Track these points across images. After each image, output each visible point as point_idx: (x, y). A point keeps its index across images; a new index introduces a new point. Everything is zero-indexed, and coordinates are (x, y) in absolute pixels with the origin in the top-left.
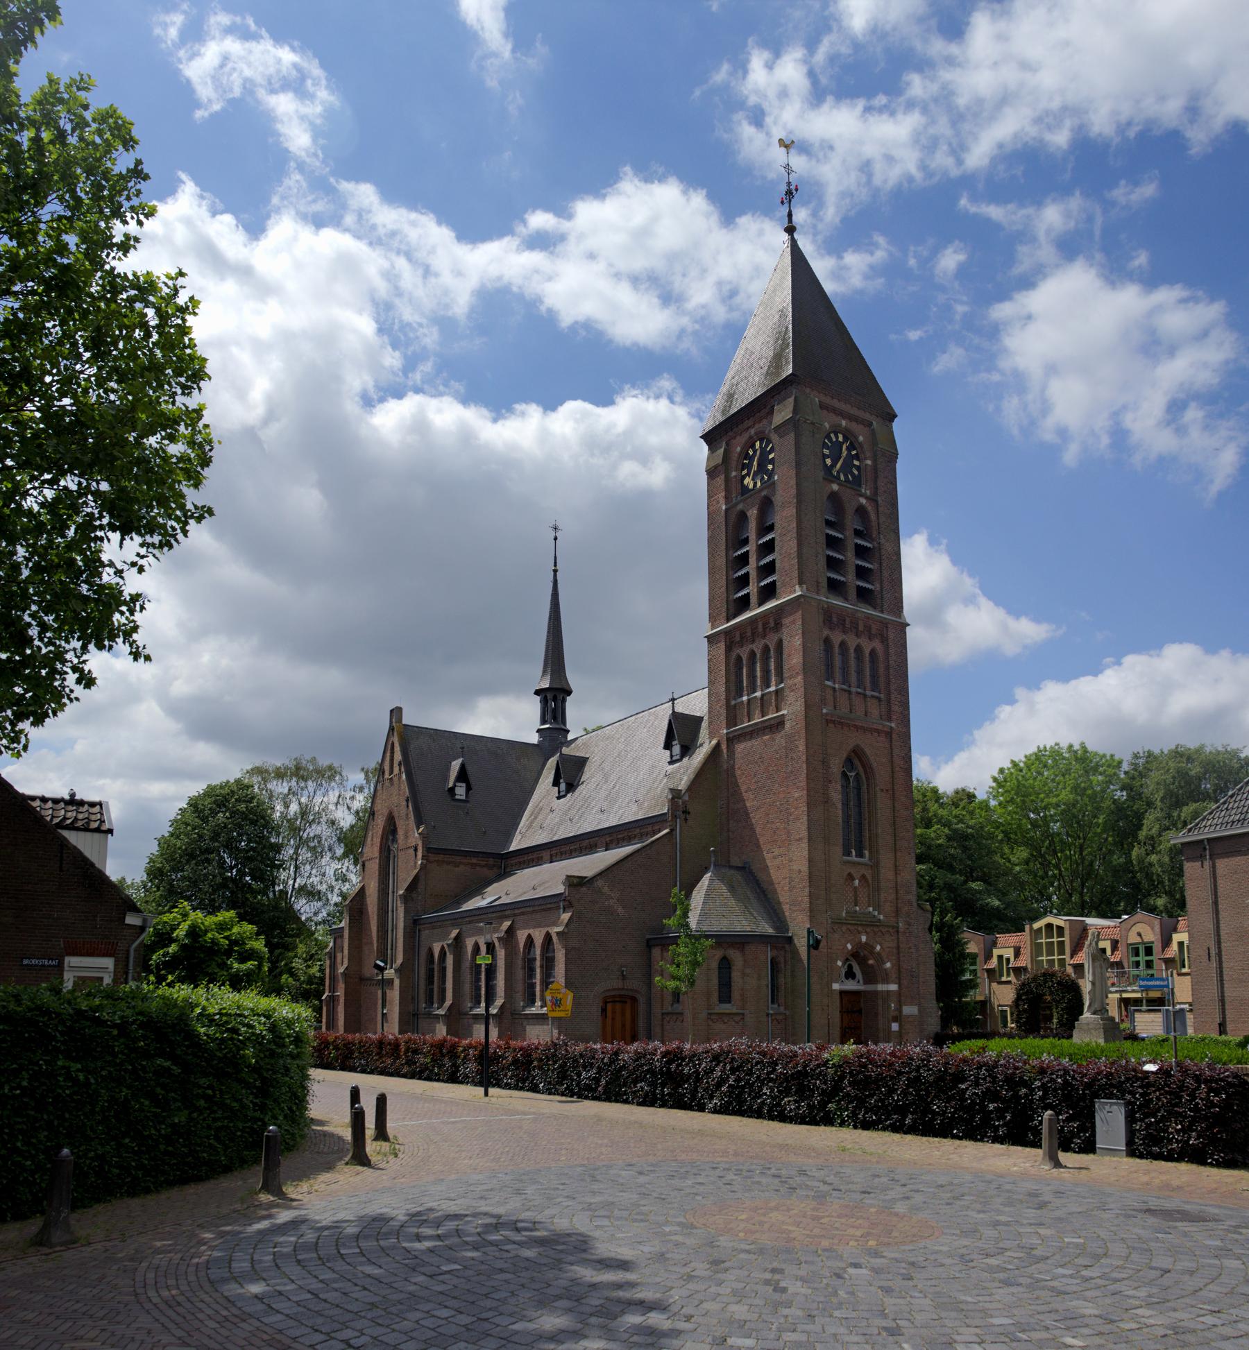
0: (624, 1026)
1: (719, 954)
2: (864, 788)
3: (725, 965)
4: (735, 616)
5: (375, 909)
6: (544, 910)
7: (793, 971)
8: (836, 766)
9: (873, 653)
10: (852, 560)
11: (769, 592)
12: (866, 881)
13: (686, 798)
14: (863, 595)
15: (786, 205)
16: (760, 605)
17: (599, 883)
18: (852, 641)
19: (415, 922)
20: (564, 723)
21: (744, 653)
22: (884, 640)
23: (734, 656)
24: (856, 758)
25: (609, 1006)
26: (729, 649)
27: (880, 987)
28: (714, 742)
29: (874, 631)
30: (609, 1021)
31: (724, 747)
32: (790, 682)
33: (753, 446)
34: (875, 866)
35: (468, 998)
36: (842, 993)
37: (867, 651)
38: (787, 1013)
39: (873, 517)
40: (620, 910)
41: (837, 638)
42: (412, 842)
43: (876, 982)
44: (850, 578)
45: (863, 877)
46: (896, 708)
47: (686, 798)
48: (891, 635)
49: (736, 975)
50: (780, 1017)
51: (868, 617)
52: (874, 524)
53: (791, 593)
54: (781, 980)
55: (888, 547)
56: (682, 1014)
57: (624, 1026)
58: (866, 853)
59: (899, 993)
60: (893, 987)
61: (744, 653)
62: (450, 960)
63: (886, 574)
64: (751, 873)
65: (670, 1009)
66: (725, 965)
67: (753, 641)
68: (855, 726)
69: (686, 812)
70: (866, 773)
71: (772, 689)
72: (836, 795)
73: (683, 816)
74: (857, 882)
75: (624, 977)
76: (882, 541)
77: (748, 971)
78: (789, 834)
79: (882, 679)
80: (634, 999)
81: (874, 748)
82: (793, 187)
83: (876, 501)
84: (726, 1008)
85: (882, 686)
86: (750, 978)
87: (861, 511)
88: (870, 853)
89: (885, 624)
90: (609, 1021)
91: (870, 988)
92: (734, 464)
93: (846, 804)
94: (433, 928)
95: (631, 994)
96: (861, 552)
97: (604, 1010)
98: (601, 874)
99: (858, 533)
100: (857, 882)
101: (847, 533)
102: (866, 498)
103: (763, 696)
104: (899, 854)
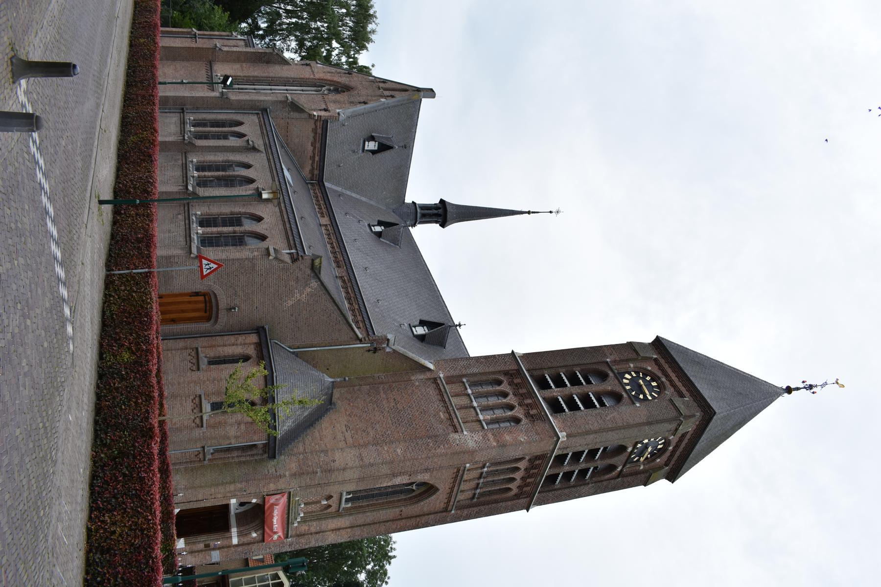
0: (183, 311)
2: (403, 497)
4: (531, 376)
5: (272, 75)
6: (286, 233)
7: (244, 462)
9: (510, 489)
11: (556, 407)
13: (388, 350)
15: (802, 385)
16: (544, 399)
17: (314, 284)
18: (518, 475)
19: (265, 110)
20: (421, 223)
21: (505, 387)
22: (517, 496)
23: (502, 378)
25: (201, 298)
26: (506, 373)
27: (234, 531)
28: (431, 366)
30: (186, 299)
31: (428, 375)
32: (490, 436)
33: (653, 380)
34: (338, 514)
35: (201, 159)
36: (227, 506)
38: (206, 462)
40: (290, 303)
42: (331, 107)
43: (239, 525)
44: (566, 468)
45: (329, 506)
46: (466, 512)
50: (201, 456)
52: (603, 478)
53: (559, 428)
54: (235, 454)
55: (585, 489)
56: (198, 369)
57: (183, 311)
58: (350, 505)
59: (230, 546)
60: (235, 541)
61: (505, 387)
62: (233, 142)
64: (327, 410)
65: (201, 355)
67: (515, 395)
69: (375, 350)
70: (416, 497)
71: (481, 417)
75: (229, 309)
76: (590, 485)
77: (243, 427)
78: (365, 445)
79: (488, 498)
80: (209, 319)
81: (436, 501)
82: (814, 390)
83: (618, 477)
85: (482, 499)
87: (613, 467)
90: (186, 299)
91: (233, 520)
92: (639, 365)
94: (261, 126)
95: (214, 315)
96: (583, 473)
97: (197, 294)
98: (322, 284)
99: (595, 468)
102: (622, 470)
103: (474, 408)
104: (349, 530)
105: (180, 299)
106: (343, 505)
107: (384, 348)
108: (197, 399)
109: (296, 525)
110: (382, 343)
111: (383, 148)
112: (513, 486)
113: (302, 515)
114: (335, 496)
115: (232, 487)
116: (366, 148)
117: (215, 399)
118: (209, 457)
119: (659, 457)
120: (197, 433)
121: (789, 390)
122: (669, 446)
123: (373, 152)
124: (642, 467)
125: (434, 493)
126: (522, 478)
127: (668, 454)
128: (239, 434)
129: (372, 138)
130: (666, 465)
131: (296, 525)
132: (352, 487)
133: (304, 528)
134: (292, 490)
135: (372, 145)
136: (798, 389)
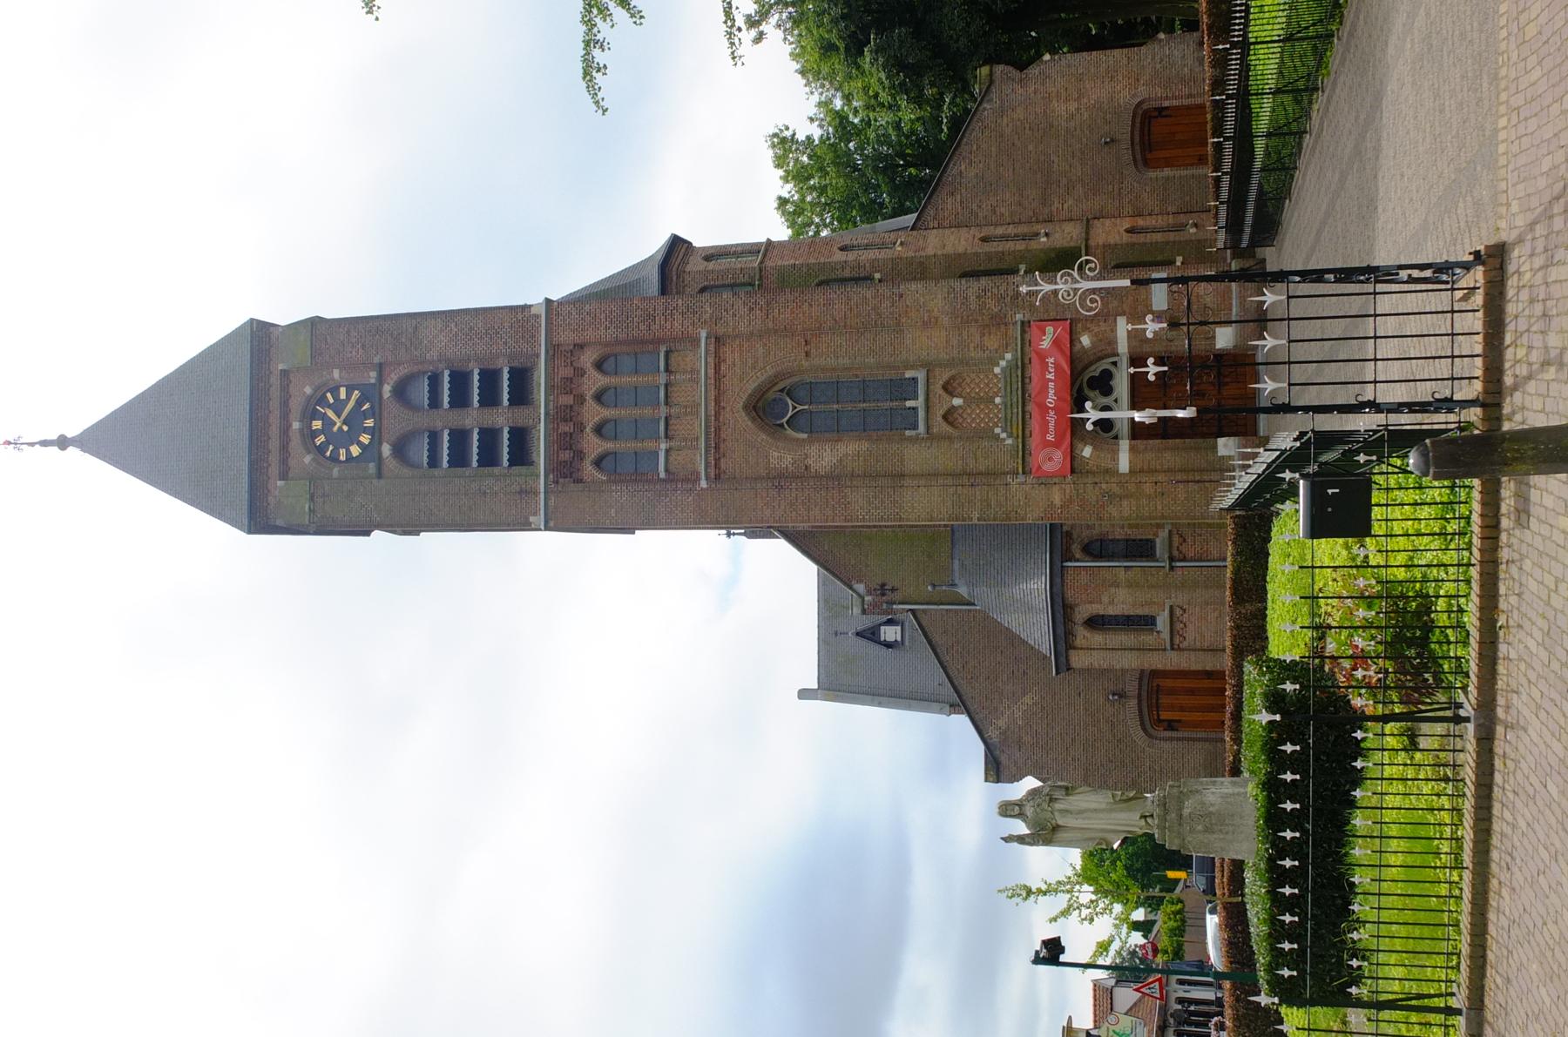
1: (1083, 636)
3: (1095, 623)
8: (781, 457)
12: (953, 378)
13: (861, 588)
14: (521, 395)
18: (593, 413)
22: (581, 347)
24: (763, 408)
25: (1164, 715)
29: (569, 372)
37: (601, 380)
39: (404, 371)
40: (1027, 699)
41: (593, 445)
47: (861, 588)
48: (566, 337)
49: (1111, 611)
50: (1176, 539)
51: (550, 388)
55: (440, 348)
57: (1191, 692)
58: (909, 374)
66: (1095, 623)
68: (717, 415)
72: (824, 456)
73: (890, 596)
74: (957, 402)
77: (1105, 599)
80: (1155, 674)
83: (381, 365)
84: (1162, 622)
87: (400, 392)
88: (913, 367)
89: (554, 350)
93: (836, 429)
95: (1145, 681)
97: (1171, 725)
100: (957, 402)
101: (439, 425)
102: (381, 380)
105: (1197, 716)
106: (921, 375)
107: (869, 593)
108: (1177, 641)
109: (1008, 356)
110: (875, 605)
112: (594, 381)
113: (997, 370)
114: (940, 419)
116: (899, 628)
117: (1148, 639)
118: (1163, 534)
119: (309, 398)
120: (1180, 598)
121: (62, 443)
122: (301, 430)
124: (336, 374)
125: (750, 396)
126: (581, 399)
127: (296, 405)
128: (1113, 590)
130: (285, 373)
131: (1008, 356)
132: (917, 457)
133: (992, 342)
134: (1021, 478)
136: (44, 443)
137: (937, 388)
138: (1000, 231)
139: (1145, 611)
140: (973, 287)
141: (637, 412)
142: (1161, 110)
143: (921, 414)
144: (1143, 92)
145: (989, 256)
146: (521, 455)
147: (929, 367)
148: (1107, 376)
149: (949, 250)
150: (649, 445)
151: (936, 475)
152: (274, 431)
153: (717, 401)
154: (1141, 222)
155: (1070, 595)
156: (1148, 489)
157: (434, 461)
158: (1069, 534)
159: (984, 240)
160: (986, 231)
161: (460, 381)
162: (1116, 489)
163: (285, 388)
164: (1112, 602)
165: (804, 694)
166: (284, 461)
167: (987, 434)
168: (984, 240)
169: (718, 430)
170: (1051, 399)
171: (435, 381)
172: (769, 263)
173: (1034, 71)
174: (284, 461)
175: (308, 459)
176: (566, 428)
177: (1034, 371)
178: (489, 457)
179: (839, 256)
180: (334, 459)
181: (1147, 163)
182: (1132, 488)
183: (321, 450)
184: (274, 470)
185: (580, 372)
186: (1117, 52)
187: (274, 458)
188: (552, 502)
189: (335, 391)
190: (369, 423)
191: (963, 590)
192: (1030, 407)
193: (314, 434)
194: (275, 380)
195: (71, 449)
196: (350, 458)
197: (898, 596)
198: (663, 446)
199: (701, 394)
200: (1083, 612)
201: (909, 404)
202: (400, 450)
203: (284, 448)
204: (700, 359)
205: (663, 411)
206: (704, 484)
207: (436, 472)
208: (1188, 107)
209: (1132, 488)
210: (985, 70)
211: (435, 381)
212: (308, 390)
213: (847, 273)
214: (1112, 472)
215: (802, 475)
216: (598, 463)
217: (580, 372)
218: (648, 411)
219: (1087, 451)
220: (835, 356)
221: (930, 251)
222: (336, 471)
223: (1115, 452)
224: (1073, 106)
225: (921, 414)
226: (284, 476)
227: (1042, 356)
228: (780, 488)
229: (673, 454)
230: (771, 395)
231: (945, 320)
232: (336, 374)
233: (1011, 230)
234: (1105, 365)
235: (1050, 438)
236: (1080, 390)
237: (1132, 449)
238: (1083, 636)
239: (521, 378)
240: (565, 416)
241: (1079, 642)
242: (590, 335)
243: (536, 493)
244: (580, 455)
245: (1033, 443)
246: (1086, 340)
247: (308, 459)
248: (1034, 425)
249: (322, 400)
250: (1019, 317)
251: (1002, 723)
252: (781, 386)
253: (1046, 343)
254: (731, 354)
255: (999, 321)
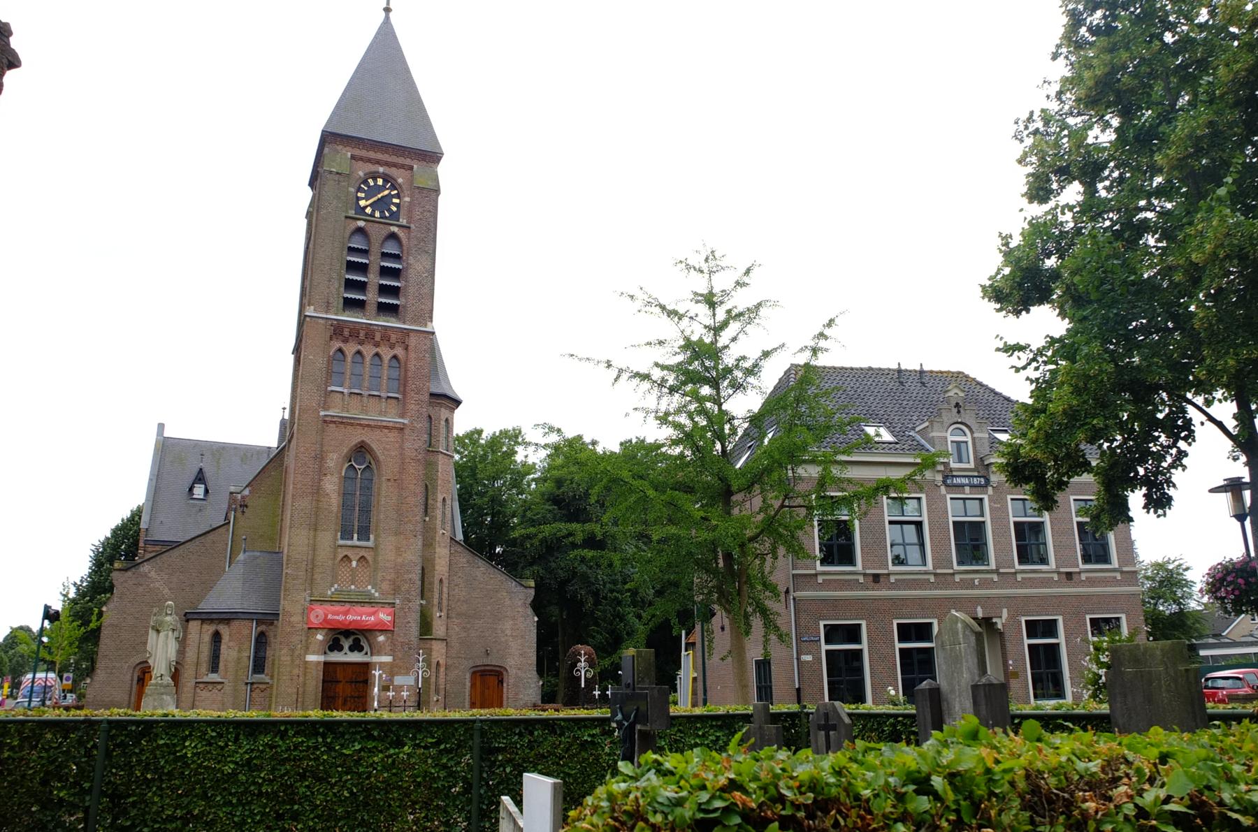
3: (217, 637)
8: (333, 460)
10: (373, 279)
13: (246, 492)
14: (384, 309)
18: (369, 351)
22: (406, 348)
24: (362, 450)
29: (393, 339)
39: (404, 241)
41: (350, 348)
47: (246, 492)
48: (413, 341)
49: (223, 647)
63: (411, 290)
66: (217, 637)
68: (360, 425)
72: (331, 485)
73: (240, 510)
74: (354, 564)
76: (411, 260)
77: (231, 644)
84: (214, 677)
86: (237, 650)
87: (393, 236)
88: (376, 539)
93: (346, 495)
100: (354, 564)
101: (372, 258)
106: (370, 544)
107: (243, 497)
111: (200, 478)
112: (387, 354)
115: (286, 659)
117: (204, 668)
118: (267, 679)
120: (228, 688)
121: (387, 10)
123: (207, 491)
124: (407, 199)
126: (377, 345)
127: (393, 172)
129: (191, 489)
130: (411, 168)
133: (385, 586)
134: (308, 599)
135: (199, 491)
137: (362, 553)
138: (445, 590)
139: (221, 665)
140: (416, 576)
141: (367, 377)
142: (501, 682)
143: (349, 543)
144: (512, 672)
145: (432, 583)
146: (350, 304)
147: (374, 549)
148: (360, 649)
149: (437, 561)
150: (347, 383)
151: (314, 550)
152: (379, 156)
153: (368, 426)
154: (442, 669)
155: (235, 624)
156: (296, 671)
157: (352, 250)
158: (272, 624)
159: (441, 581)
160: (446, 582)
161: (395, 274)
162: (297, 653)
163: (402, 166)
164: (229, 647)
165: (161, 427)
166: (361, 159)
167: (335, 579)
168: (441, 581)
169: (352, 424)
170: (350, 617)
171: (397, 257)
172: (441, 456)
173: (530, 611)
174: (361, 159)
175: (361, 173)
176: (362, 334)
177: (368, 609)
178: (350, 285)
179: (440, 498)
180: (359, 189)
181: (474, 673)
182: (297, 662)
183: (365, 182)
184: (357, 152)
185: (392, 347)
186: (534, 658)
187: (363, 153)
188: (321, 321)
189: (398, 196)
190: (377, 214)
191: (241, 557)
192: (347, 606)
193: (375, 179)
194: (408, 162)
195: (383, 14)
196: (358, 199)
197: (239, 514)
198: (346, 391)
199: (373, 416)
200: (224, 630)
201: (355, 536)
202: (360, 230)
203: (369, 160)
204: (392, 418)
205: (366, 393)
206: (322, 413)
207: (345, 252)
208: (502, 697)
209: (297, 662)
210: (532, 584)
211: (397, 257)
212: (400, 180)
213: (430, 501)
214: (307, 650)
215: (322, 472)
216: (340, 350)
217: (392, 347)
218: (366, 384)
219: (320, 637)
220: (386, 498)
221: (438, 550)
222: (352, 190)
223: (318, 653)
224: (508, 632)
225: (349, 543)
226: (353, 157)
227: (374, 613)
228: (315, 458)
229: (340, 396)
230: (368, 456)
231: (400, 560)
232: (407, 199)
233: (445, 596)
234: (366, 648)
235: (330, 617)
236: (354, 634)
237: (319, 662)
238: (209, 629)
239: (392, 310)
240: (369, 333)
241: (206, 627)
242: (412, 355)
243: (326, 312)
244: (346, 341)
245: (327, 606)
246: (381, 638)
247: (361, 173)
248: (337, 608)
249: (393, 187)
250: (398, 601)
251: (153, 573)
252: (374, 466)
253: (382, 616)
254: (393, 436)
255: (396, 590)
